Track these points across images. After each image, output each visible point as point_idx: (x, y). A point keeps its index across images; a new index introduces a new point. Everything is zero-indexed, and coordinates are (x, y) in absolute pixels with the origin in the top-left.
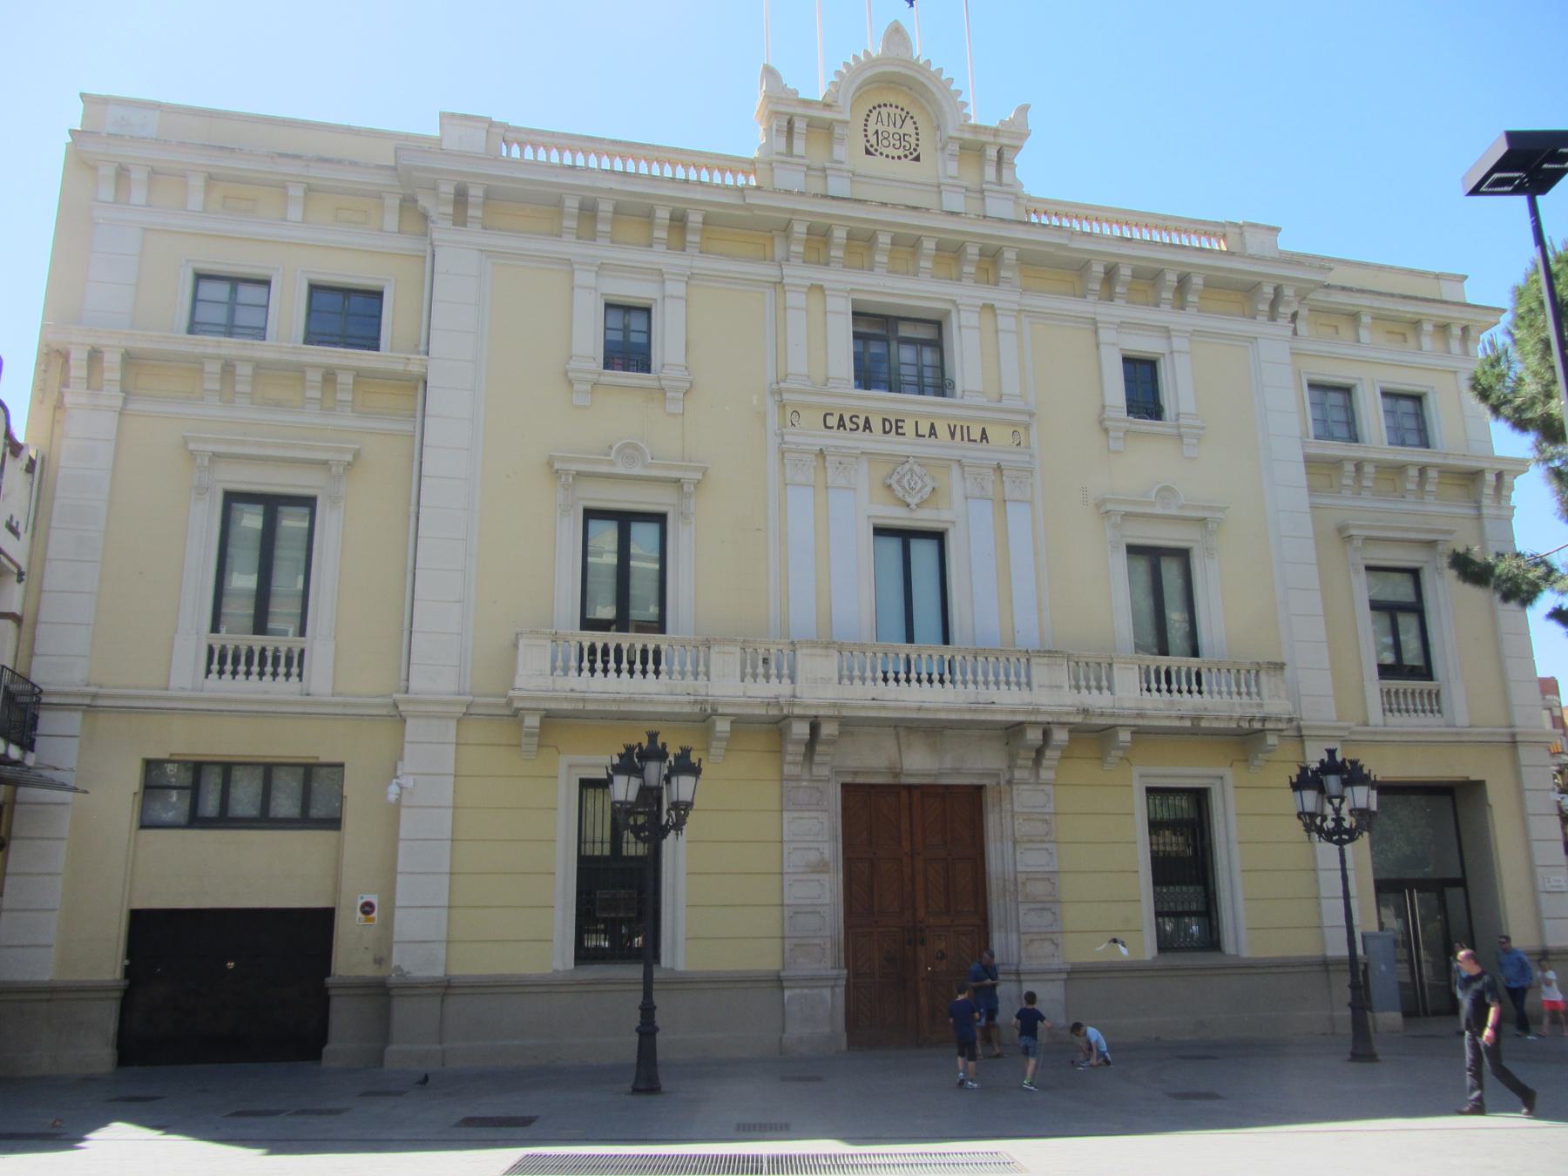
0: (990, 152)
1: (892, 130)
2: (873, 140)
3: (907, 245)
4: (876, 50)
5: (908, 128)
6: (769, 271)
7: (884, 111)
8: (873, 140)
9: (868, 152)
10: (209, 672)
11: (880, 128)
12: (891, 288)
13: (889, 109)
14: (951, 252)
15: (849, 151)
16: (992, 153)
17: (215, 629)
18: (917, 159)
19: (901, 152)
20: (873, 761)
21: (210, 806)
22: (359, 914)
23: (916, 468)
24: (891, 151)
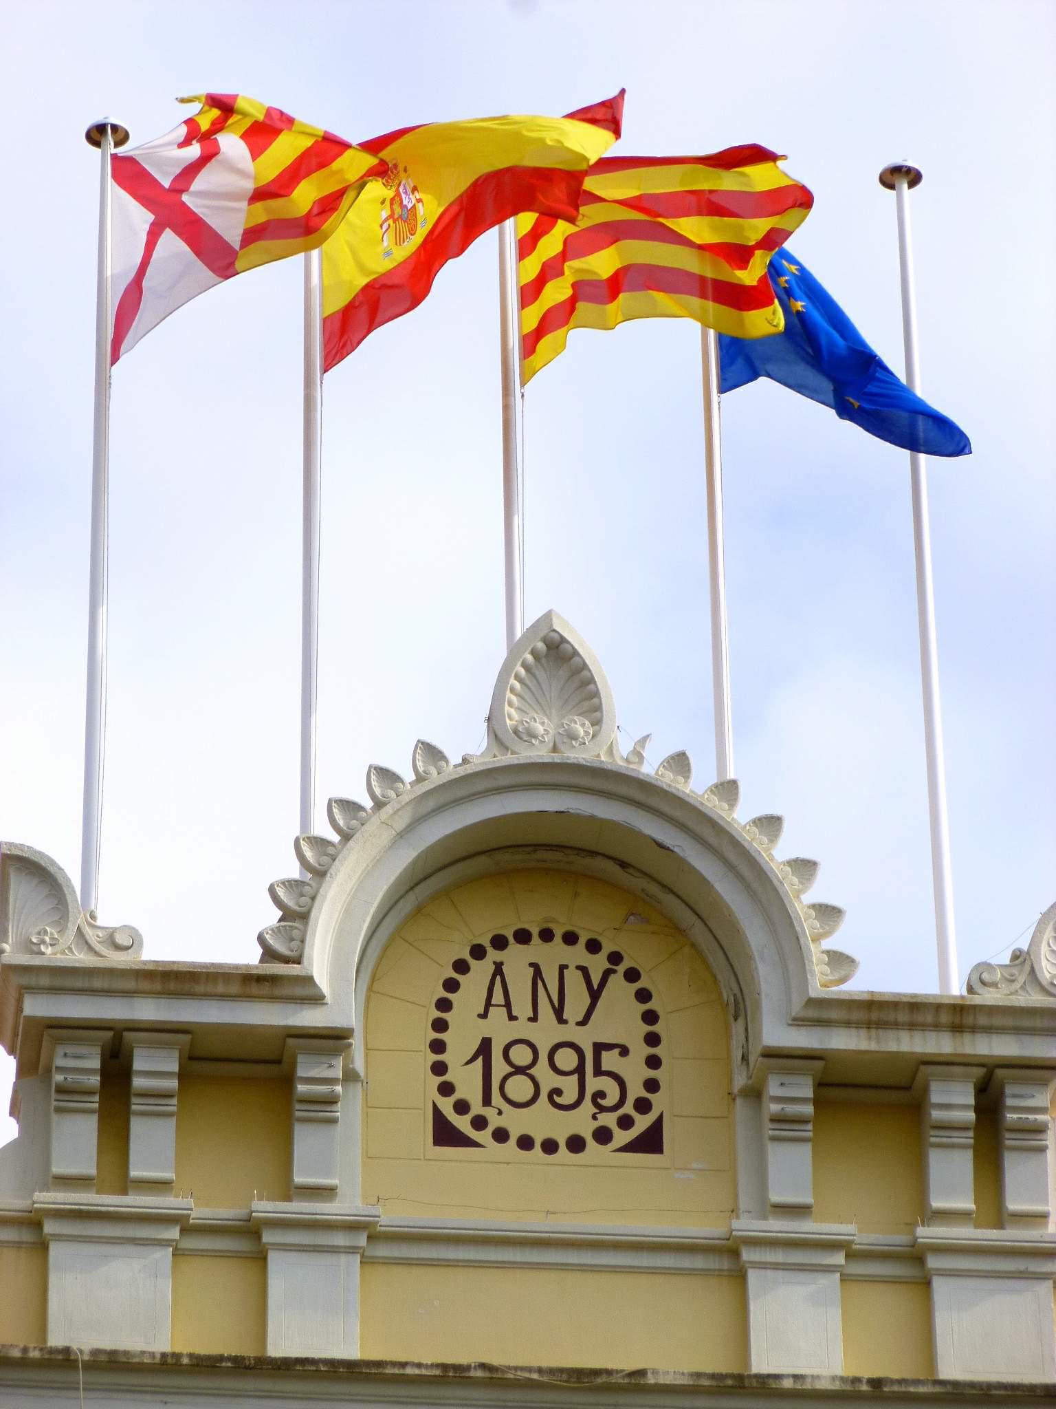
1: (546, 1033)
2: (468, 1083)
4: (465, 743)
5: (619, 1017)
7: (517, 960)
8: (468, 1083)
9: (445, 1134)
11: (500, 1030)
13: (537, 951)
15: (360, 1155)
16: (954, 1101)
18: (651, 1142)
19: (582, 1122)
24: (543, 1122)
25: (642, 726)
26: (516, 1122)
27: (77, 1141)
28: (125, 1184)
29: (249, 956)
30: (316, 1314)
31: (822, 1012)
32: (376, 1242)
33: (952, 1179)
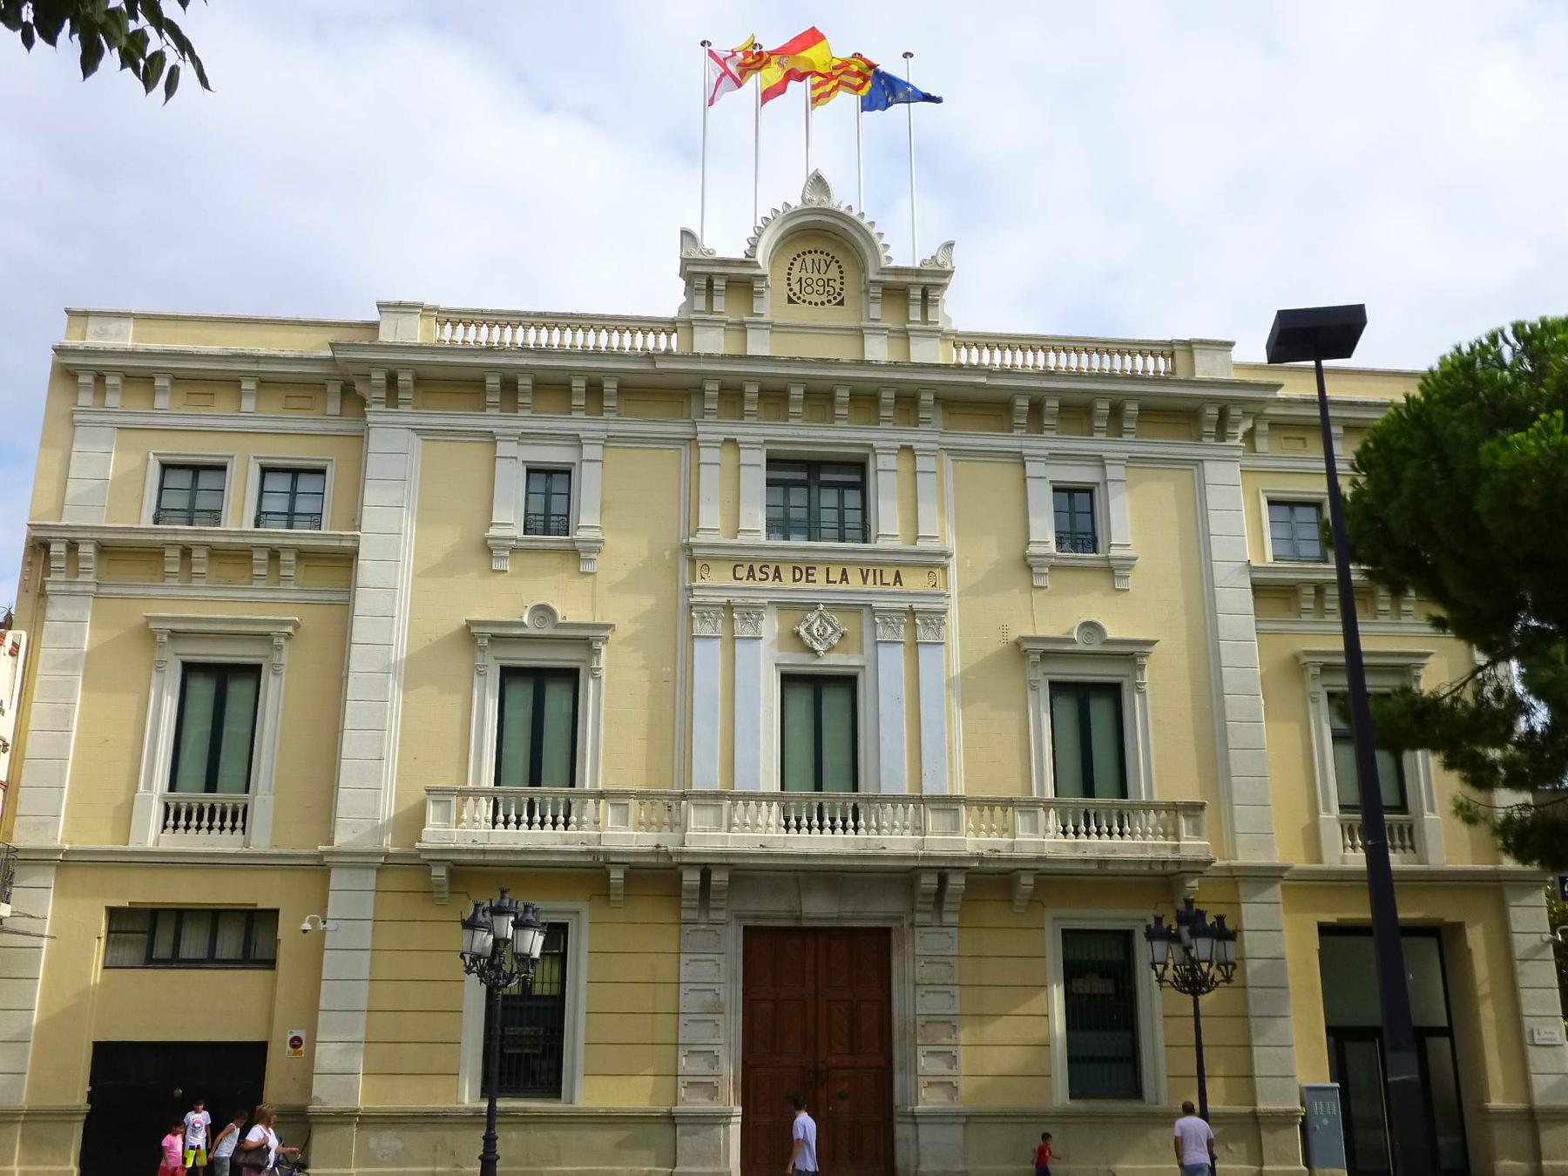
0: (915, 291)
1: (816, 276)
2: (796, 288)
3: (820, 398)
4: (796, 202)
5: (833, 272)
7: (808, 258)
8: (796, 288)
9: (791, 301)
10: (165, 827)
11: (804, 275)
12: (805, 434)
13: (813, 255)
14: (866, 400)
15: (769, 306)
16: (916, 293)
17: (172, 788)
18: (841, 303)
19: (824, 298)
21: (162, 950)
22: (289, 1048)
23: (827, 615)
24: (815, 298)
25: (842, 197)
26: (808, 298)
27: (700, 302)
29: (742, 256)
30: (758, 345)
31: (884, 271)
32: (773, 327)
33: (915, 313)
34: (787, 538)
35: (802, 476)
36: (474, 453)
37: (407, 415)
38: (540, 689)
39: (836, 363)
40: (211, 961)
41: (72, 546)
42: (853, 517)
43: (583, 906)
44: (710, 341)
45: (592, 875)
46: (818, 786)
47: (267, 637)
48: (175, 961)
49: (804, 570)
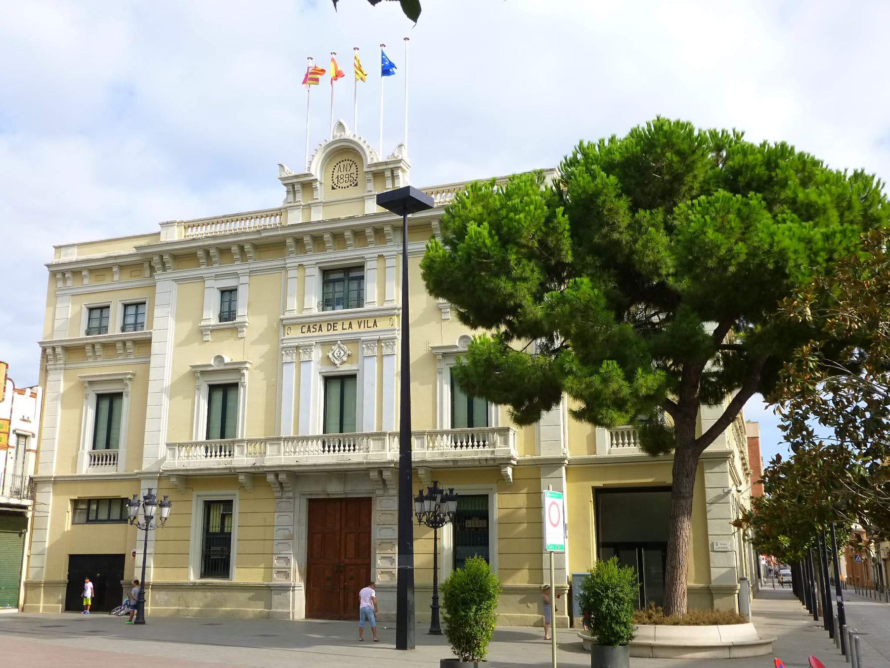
2: (336, 181)
3: (338, 237)
5: (353, 169)
6: (279, 263)
9: (333, 188)
13: (345, 163)
14: (359, 234)
15: (321, 194)
16: (388, 174)
17: (94, 448)
18: (356, 185)
19: (348, 184)
20: (318, 490)
21: (92, 516)
26: (341, 185)
27: (291, 196)
28: (295, 202)
30: (317, 215)
31: (370, 166)
32: (325, 204)
34: (333, 309)
35: (341, 275)
36: (196, 286)
37: (171, 274)
38: (223, 391)
39: (339, 220)
40: (109, 521)
41: (54, 349)
42: (354, 295)
43: (237, 492)
44: (295, 217)
45: (229, 477)
46: (341, 431)
47: (121, 380)
48: (97, 521)
49: (332, 325)
